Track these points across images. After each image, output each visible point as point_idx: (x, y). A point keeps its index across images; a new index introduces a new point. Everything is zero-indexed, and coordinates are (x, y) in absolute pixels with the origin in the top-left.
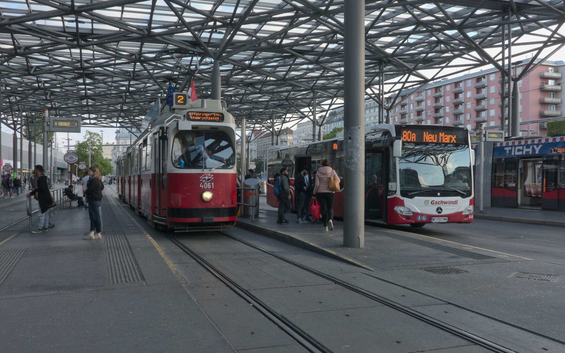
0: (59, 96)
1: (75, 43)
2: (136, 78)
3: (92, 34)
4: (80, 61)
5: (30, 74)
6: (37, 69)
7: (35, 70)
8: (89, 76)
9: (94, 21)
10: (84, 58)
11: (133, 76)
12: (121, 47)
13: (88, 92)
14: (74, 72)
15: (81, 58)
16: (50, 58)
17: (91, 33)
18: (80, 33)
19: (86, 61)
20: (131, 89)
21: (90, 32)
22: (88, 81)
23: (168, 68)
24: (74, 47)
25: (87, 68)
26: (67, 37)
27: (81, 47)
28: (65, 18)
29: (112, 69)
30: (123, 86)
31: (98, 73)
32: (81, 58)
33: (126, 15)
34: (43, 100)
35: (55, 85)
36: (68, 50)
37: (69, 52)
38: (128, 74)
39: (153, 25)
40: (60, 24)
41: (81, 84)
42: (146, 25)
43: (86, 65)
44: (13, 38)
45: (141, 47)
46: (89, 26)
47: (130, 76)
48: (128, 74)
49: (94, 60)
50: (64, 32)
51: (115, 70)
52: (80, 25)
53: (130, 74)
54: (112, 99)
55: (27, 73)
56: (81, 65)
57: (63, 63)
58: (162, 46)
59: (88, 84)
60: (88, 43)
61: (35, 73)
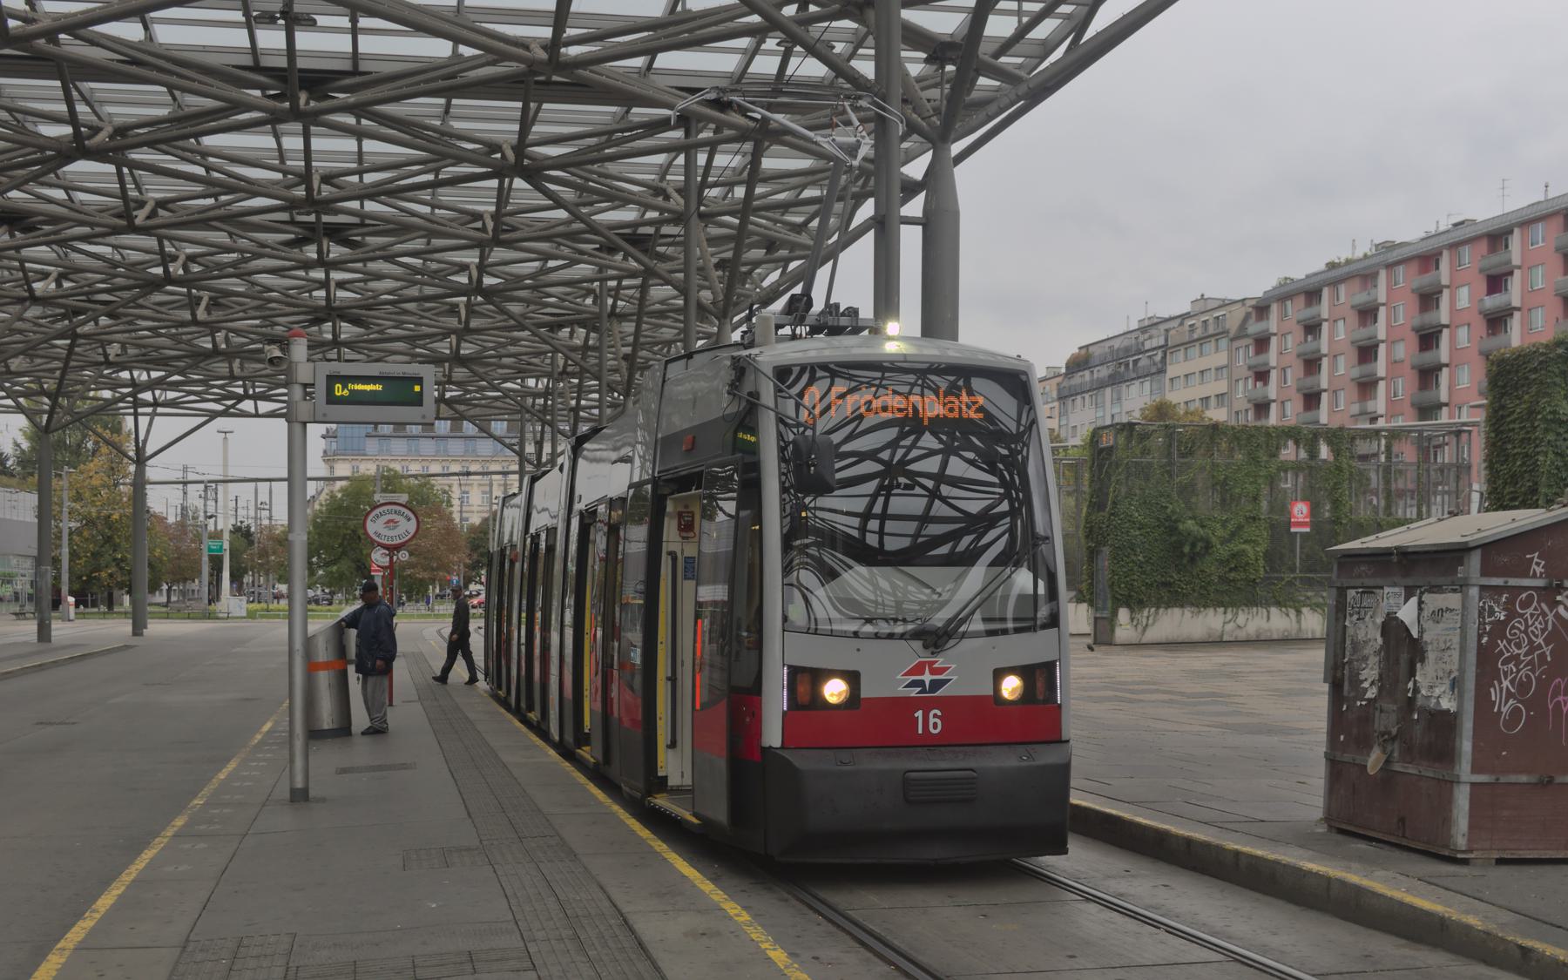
0: (239, 308)
2: (504, 236)
3: (355, 72)
4: (305, 177)
5: (133, 229)
6: (161, 212)
7: (153, 214)
8: (337, 233)
13: (341, 294)
14: (292, 222)
16: (208, 169)
19: (327, 179)
20: (488, 281)
21: (346, 66)
22: (336, 251)
26: (263, 87)
27: (309, 120)
29: (426, 210)
30: (463, 268)
34: (183, 324)
35: (221, 266)
37: (275, 146)
39: (570, 32)
41: (307, 265)
42: (547, 33)
46: (343, 44)
47: (484, 229)
48: (479, 224)
49: (360, 173)
51: (437, 211)
53: (484, 224)
54: (423, 317)
55: (123, 223)
56: (309, 189)
58: (603, 113)
61: (150, 222)
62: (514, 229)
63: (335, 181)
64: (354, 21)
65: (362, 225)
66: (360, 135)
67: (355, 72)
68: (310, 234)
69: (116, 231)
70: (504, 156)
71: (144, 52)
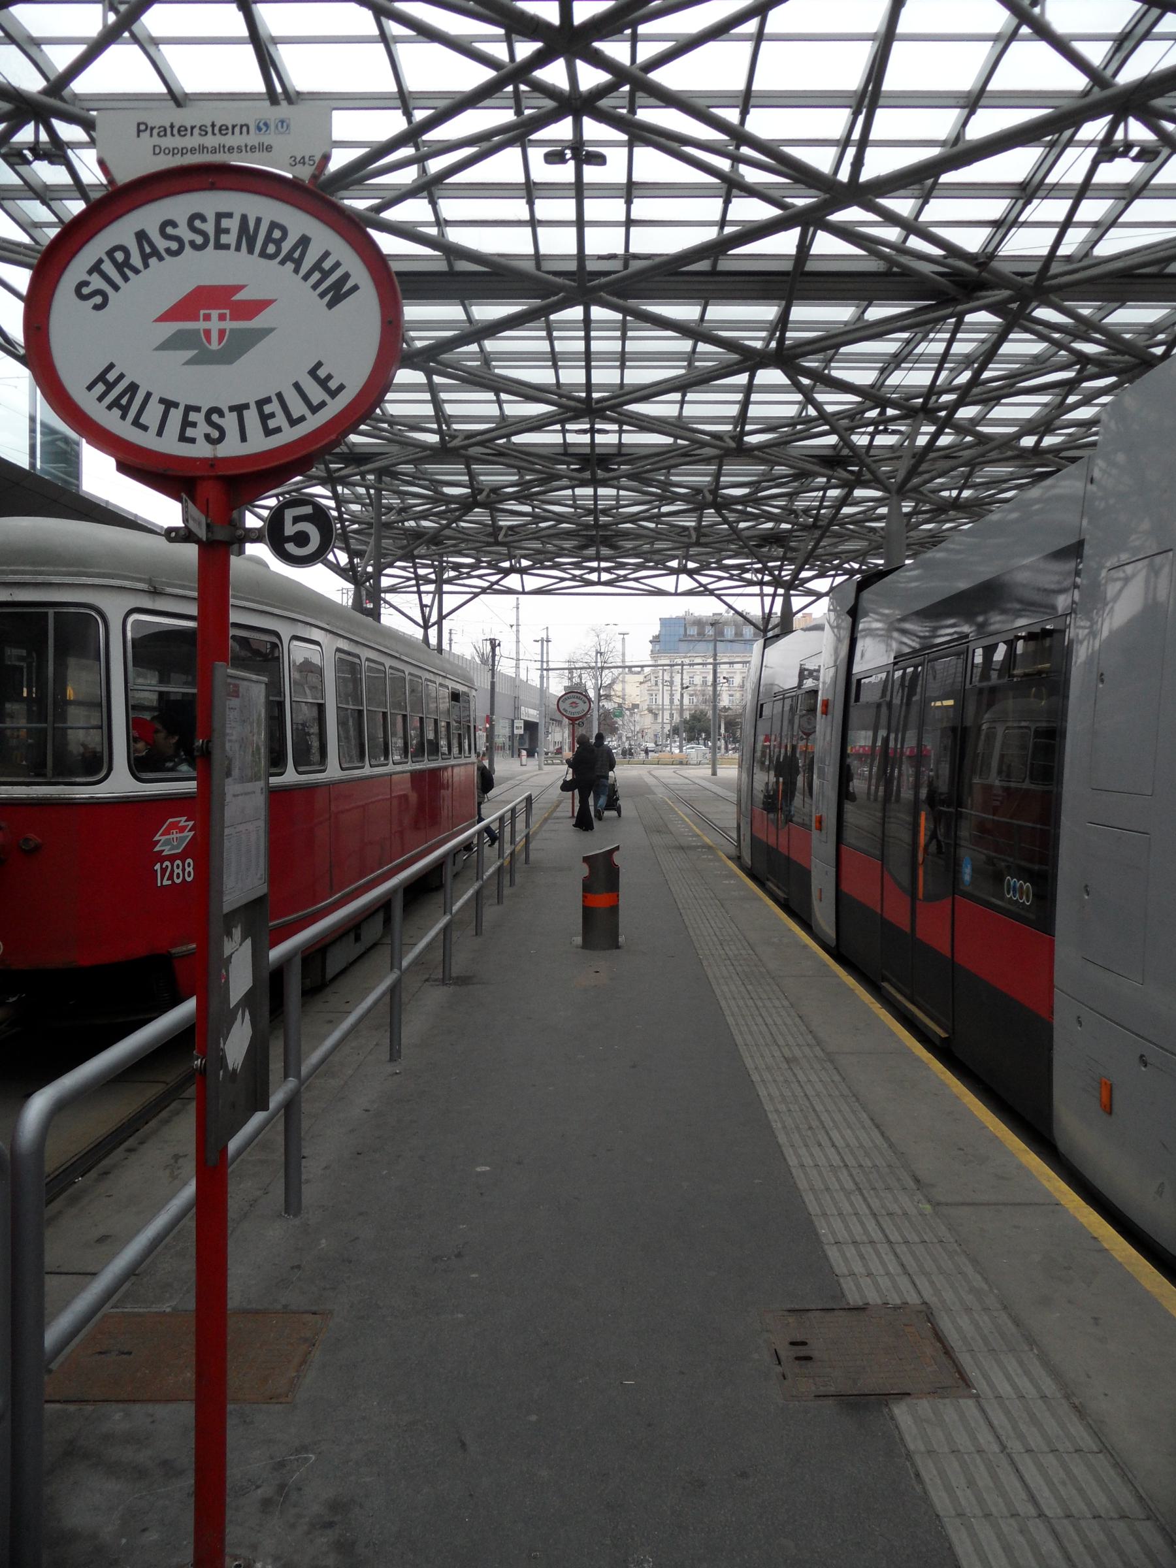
1: (587, 475)
2: (703, 540)
3: (619, 454)
5: (497, 543)
6: (510, 533)
7: (506, 535)
9: (625, 427)
10: (602, 504)
11: (698, 538)
12: (674, 478)
14: (579, 535)
15: (596, 504)
16: (534, 507)
17: (620, 453)
18: (598, 454)
19: (605, 512)
21: (614, 451)
22: (605, 551)
23: (770, 517)
24: (583, 484)
25: (606, 526)
26: (568, 464)
27: (595, 483)
28: (568, 427)
31: (626, 534)
32: (596, 504)
33: (688, 411)
36: (569, 492)
38: (686, 533)
40: (557, 439)
43: (603, 519)
44: (470, 473)
45: (718, 475)
46: (612, 439)
47: (689, 536)
48: (686, 533)
49: (617, 508)
50: (566, 454)
52: (599, 439)
53: (690, 534)
57: (560, 518)
59: (606, 560)
60: (611, 474)
62: (705, 535)
63: (608, 512)
64: (620, 427)
65: (616, 536)
66: (619, 488)
67: (619, 454)
68: (590, 542)
69: (489, 544)
70: (704, 497)
71: (509, 449)
